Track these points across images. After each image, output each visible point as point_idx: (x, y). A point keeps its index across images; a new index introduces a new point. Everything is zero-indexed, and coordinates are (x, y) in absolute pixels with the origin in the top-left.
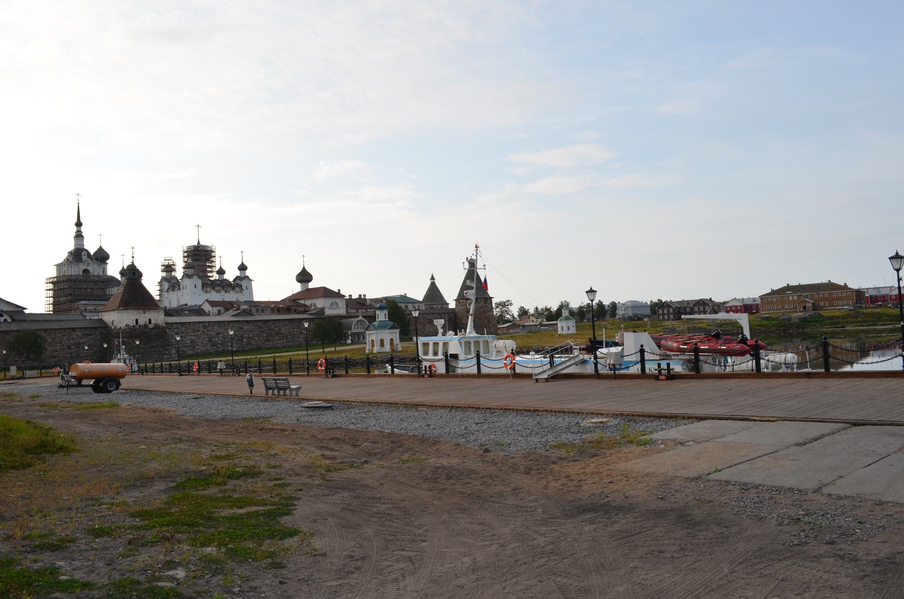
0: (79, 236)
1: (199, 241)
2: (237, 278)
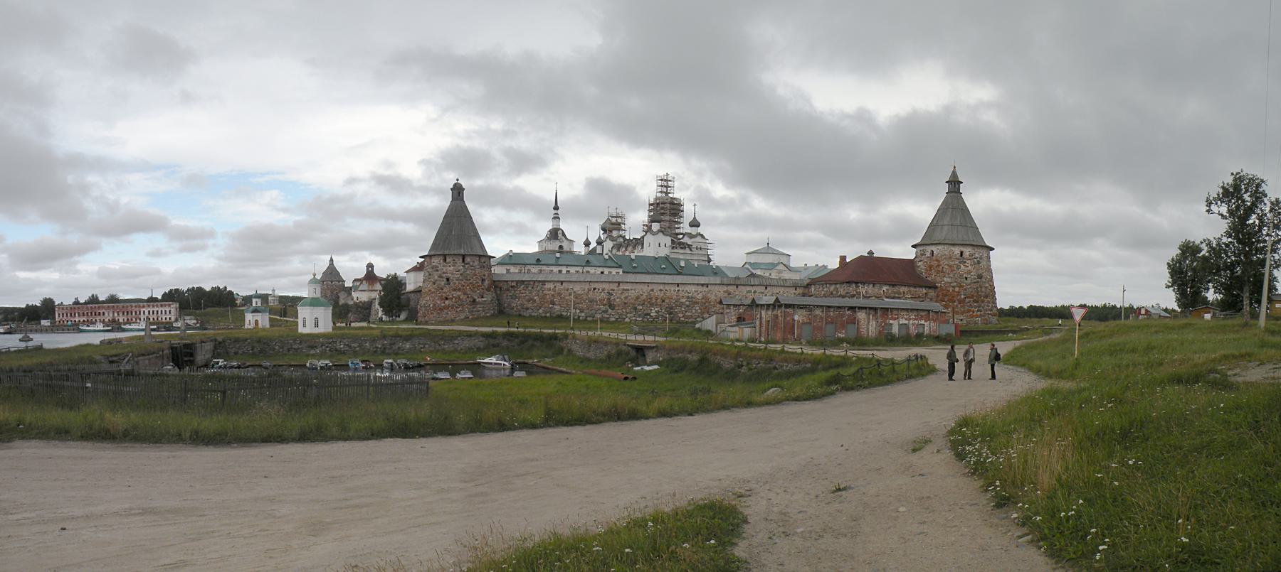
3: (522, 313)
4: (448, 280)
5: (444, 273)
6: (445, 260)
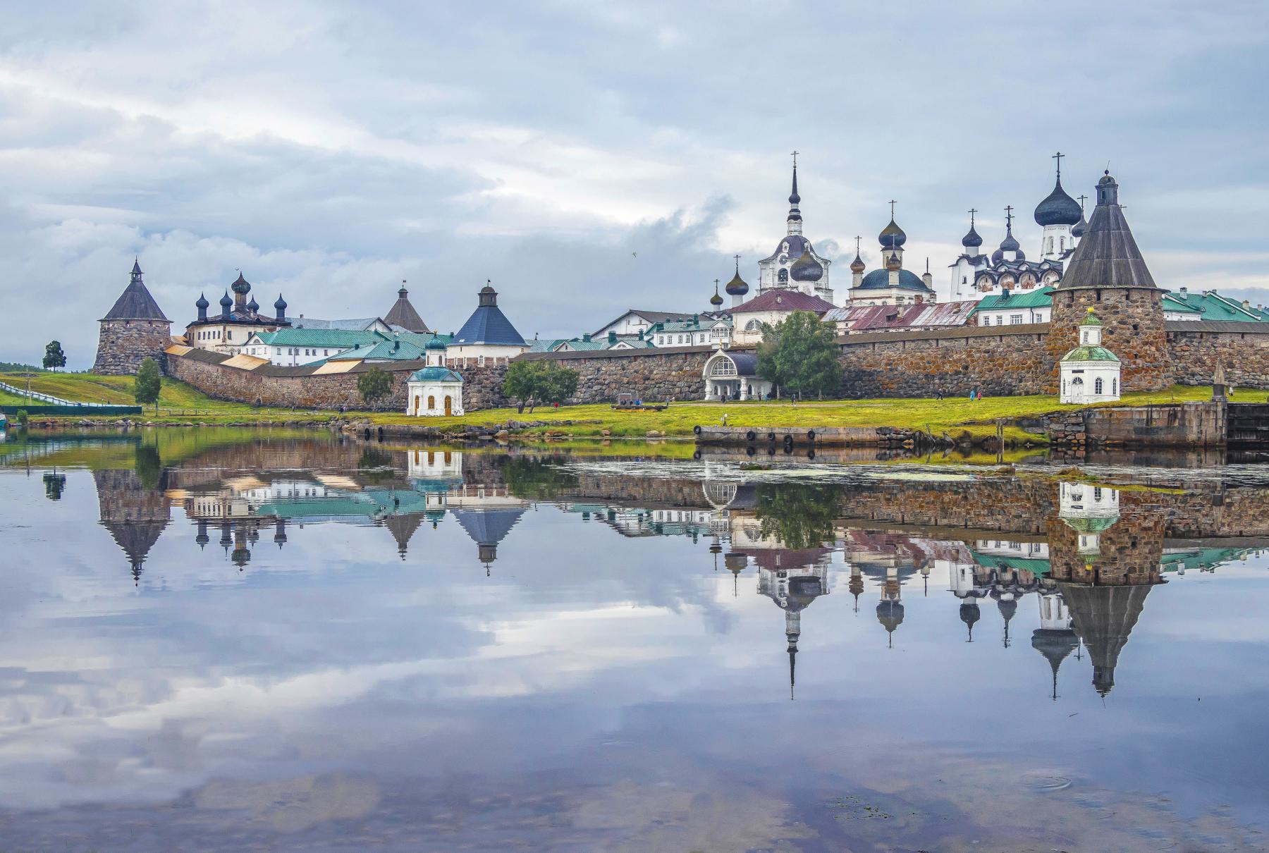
0: (795, 217)
1: (1058, 183)
3: (1186, 380)
4: (1135, 327)
5: (1129, 317)
6: (1127, 297)
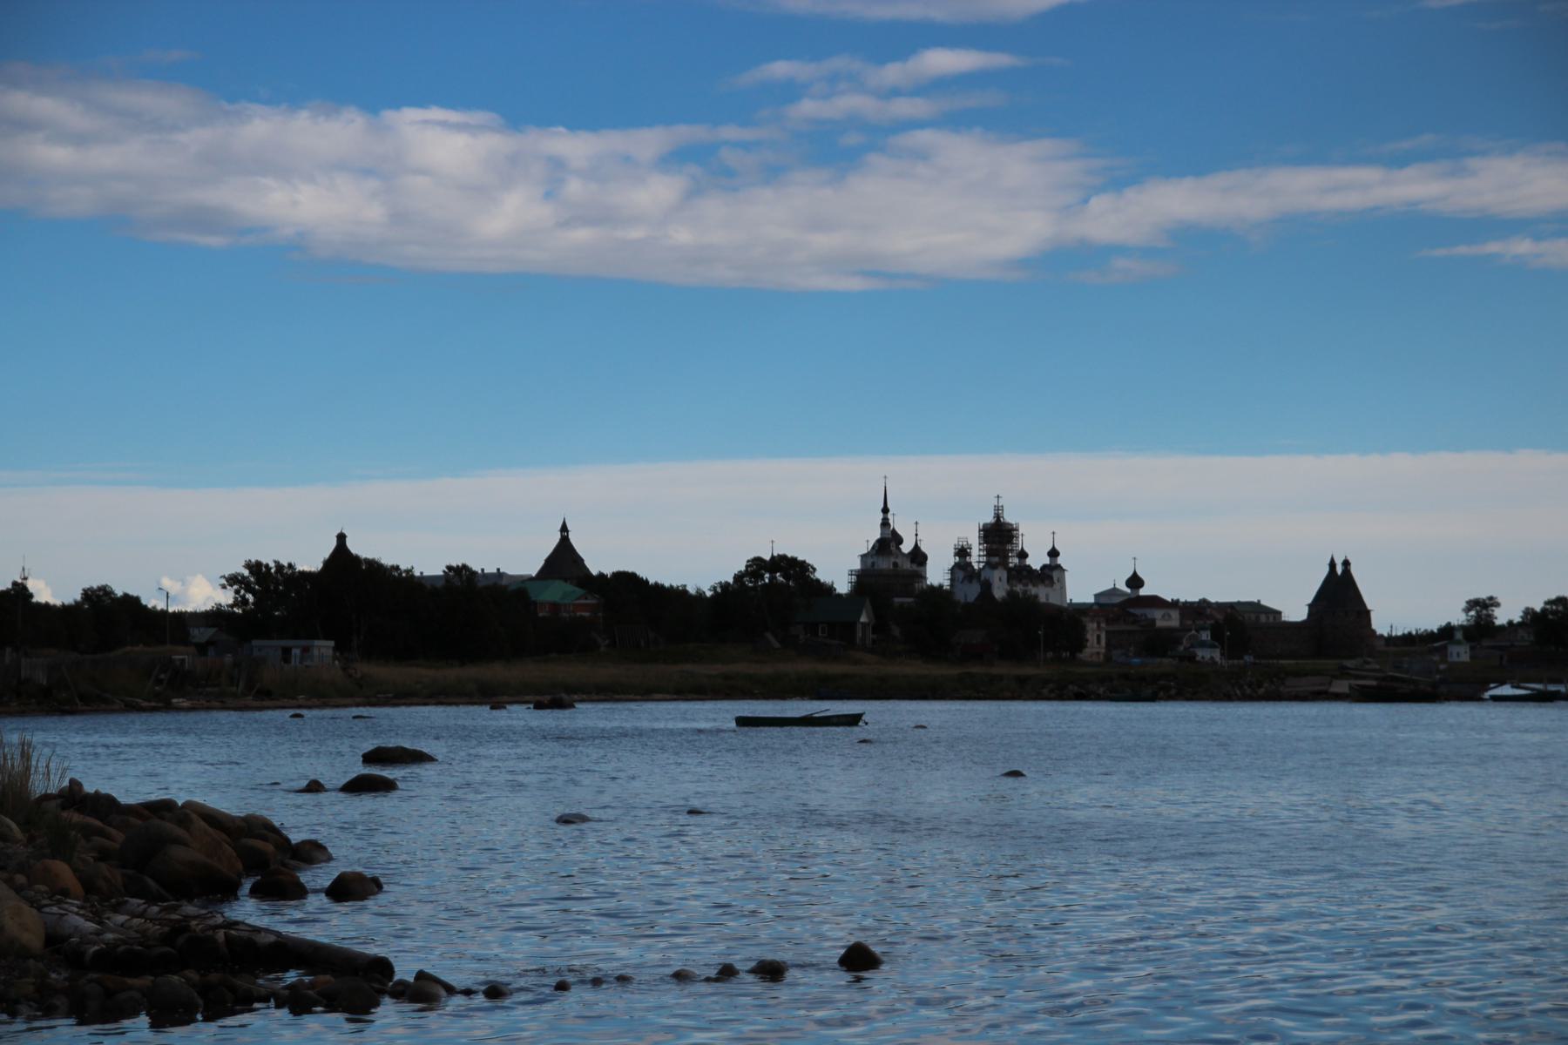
0: (885, 523)
2: (1044, 567)
